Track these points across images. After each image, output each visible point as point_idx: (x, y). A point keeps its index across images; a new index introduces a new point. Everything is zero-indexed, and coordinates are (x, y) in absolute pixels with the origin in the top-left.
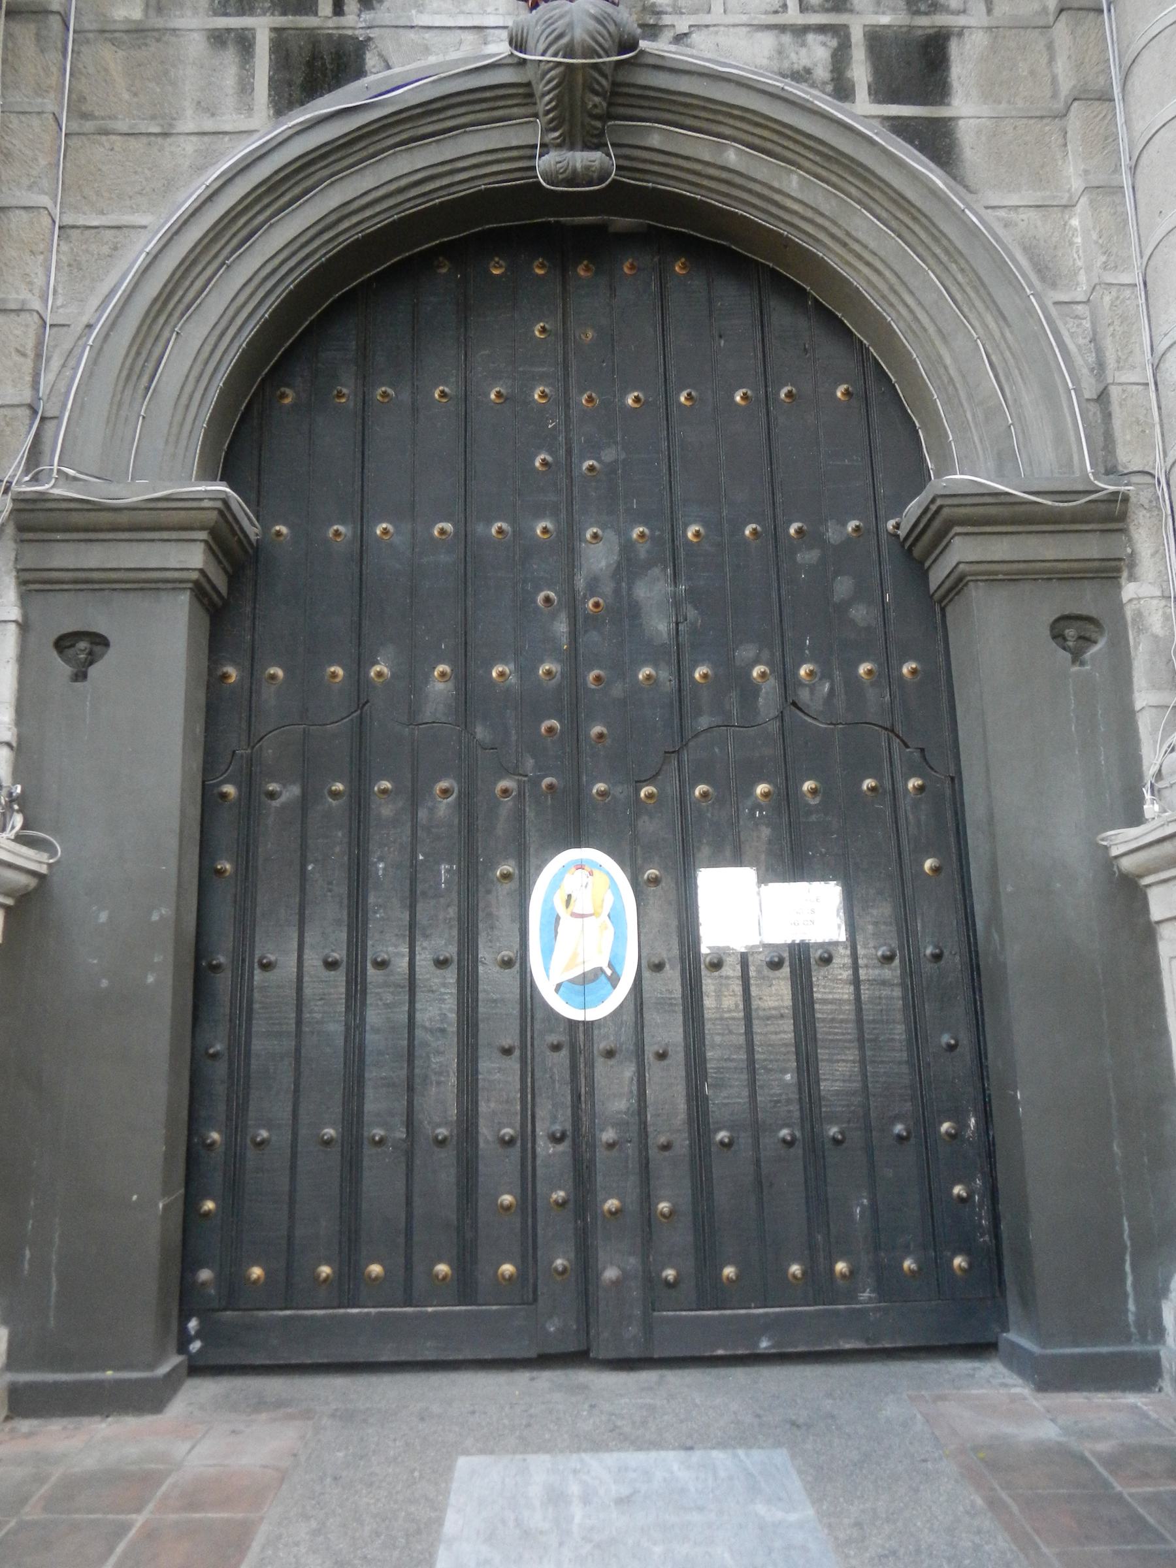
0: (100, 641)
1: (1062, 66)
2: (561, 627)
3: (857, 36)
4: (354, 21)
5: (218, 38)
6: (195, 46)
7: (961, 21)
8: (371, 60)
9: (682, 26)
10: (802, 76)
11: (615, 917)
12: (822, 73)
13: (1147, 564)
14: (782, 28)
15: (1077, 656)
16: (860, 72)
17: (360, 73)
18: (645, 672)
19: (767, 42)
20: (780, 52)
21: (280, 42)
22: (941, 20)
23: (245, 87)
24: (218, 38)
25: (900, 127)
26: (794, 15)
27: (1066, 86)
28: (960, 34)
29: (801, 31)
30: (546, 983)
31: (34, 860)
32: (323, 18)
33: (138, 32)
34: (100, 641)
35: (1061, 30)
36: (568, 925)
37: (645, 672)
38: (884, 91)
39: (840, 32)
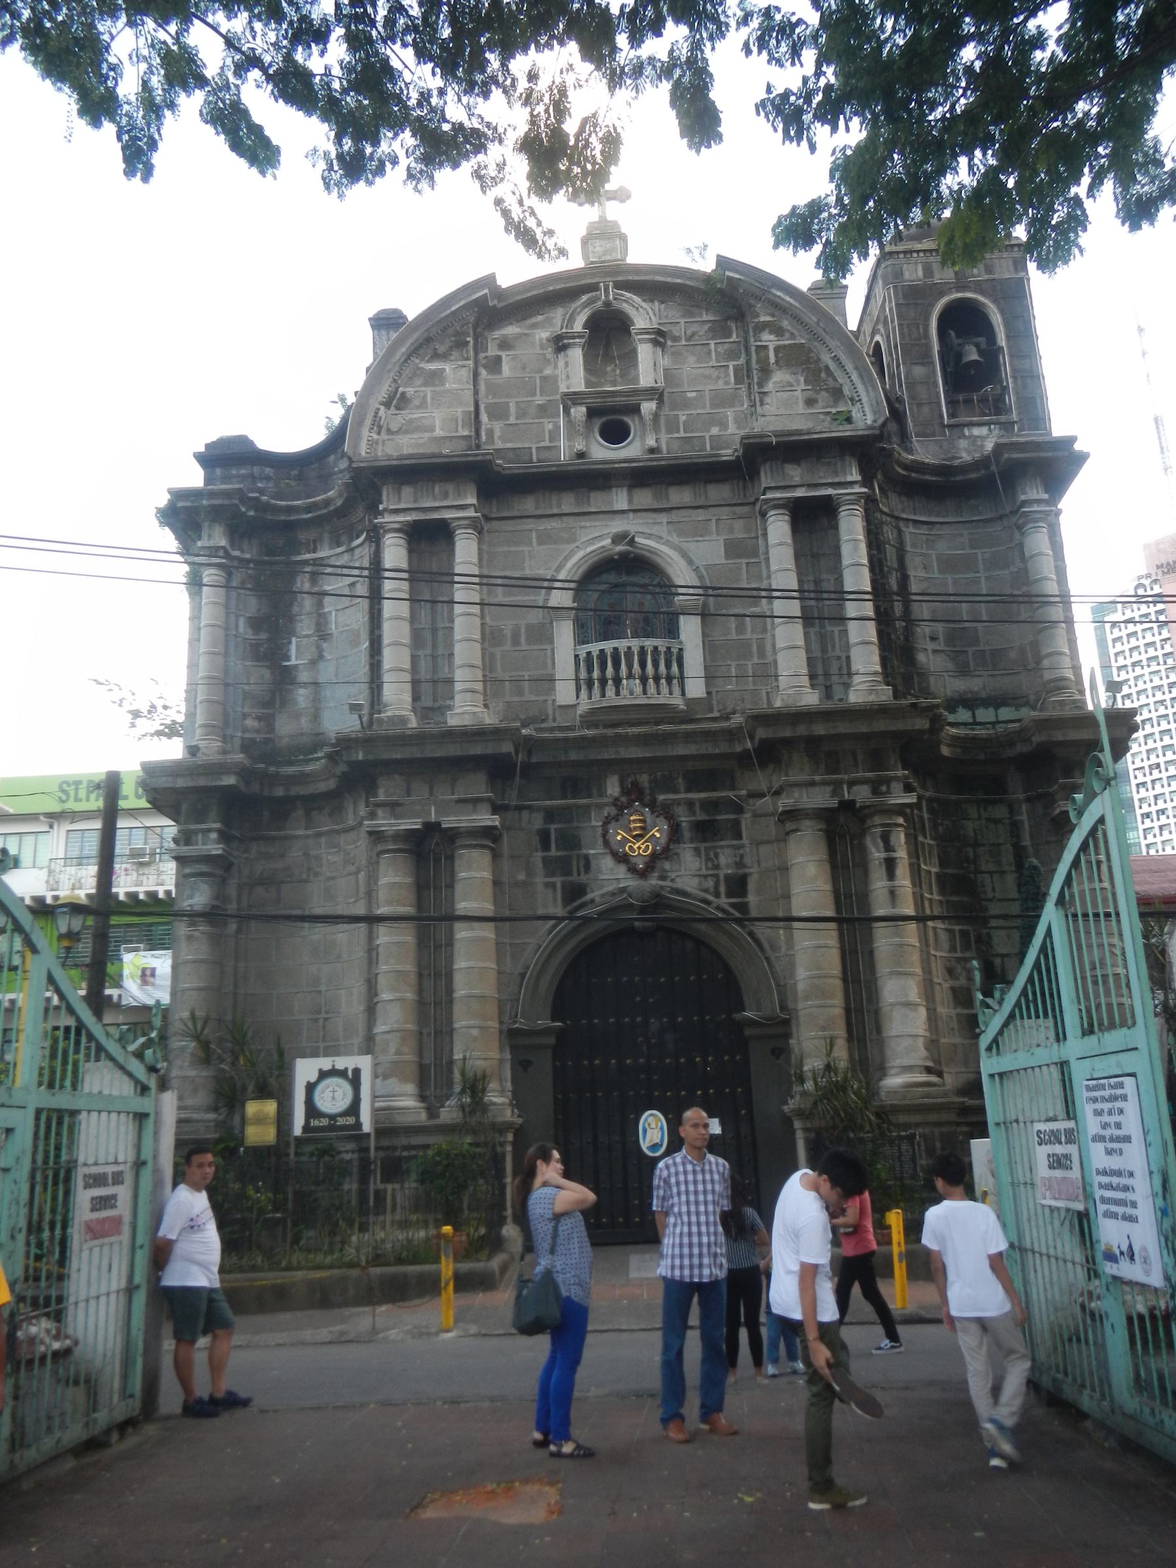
0: (529, 1063)
1: (778, 885)
2: (645, 1048)
3: (722, 877)
4: (583, 878)
5: (547, 885)
6: (540, 888)
7: (751, 870)
8: (588, 890)
9: (673, 875)
10: (706, 891)
11: (662, 1129)
12: (712, 890)
13: (795, 1034)
14: (700, 876)
15: (778, 1058)
16: (722, 889)
17: (585, 894)
18: (668, 1061)
19: (696, 881)
20: (700, 883)
21: (564, 884)
22: (746, 870)
23: (555, 900)
24: (547, 885)
25: (732, 905)
26: (704, 872)
27: (779, 892)
28: (751, 874)
29: (706, 876)
30: (644, 1146)
31: (520, 1121)
32: (574, 878)
33: (524, 883)
34: (529, 1063)
35: (778, 873)
36: (649, 1132)
37: (668, 1061)
38: (729, 895)
39: (717, 876)
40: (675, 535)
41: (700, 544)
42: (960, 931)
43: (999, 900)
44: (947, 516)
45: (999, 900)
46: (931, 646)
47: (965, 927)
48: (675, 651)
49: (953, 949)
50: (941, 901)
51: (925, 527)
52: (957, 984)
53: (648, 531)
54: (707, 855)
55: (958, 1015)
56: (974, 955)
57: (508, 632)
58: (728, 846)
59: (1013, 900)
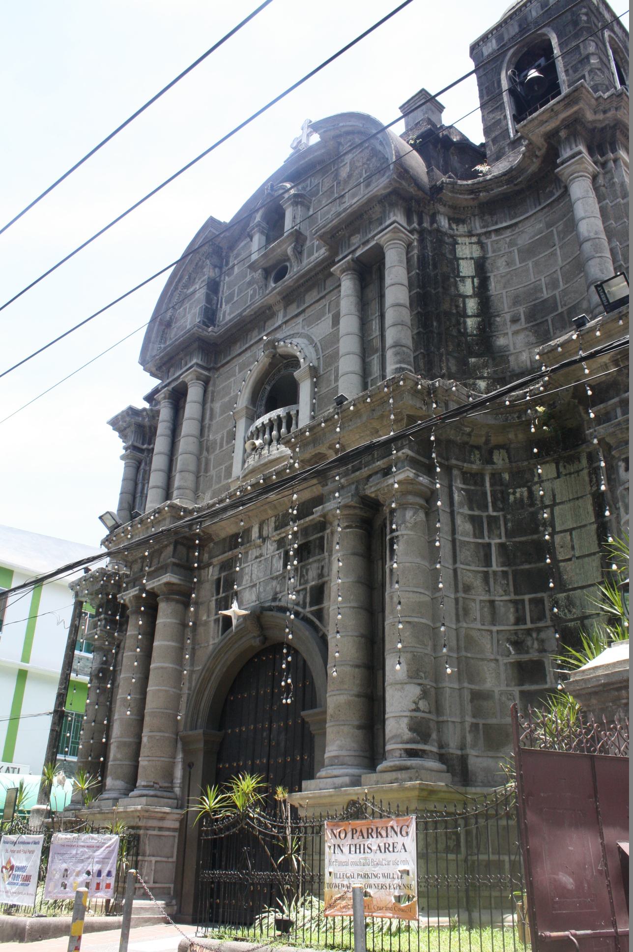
40: (306, 328)
41: (319, 325)
42: (530, 600)
43: (578, 558)
44: (528, 212)
45: (578, 558)
46: (511, 329)
47: (539, 595)
48: (293, 413)
49: (520, 620)
50: (505, 573)
51: (509, 230)
52: (525, 657)
53: (292, 332)
54: (302, 572)
55: (522, 693)
56: (549, 623)
57: (218, 441)
58: (315, 561)
59: (594, 554)
